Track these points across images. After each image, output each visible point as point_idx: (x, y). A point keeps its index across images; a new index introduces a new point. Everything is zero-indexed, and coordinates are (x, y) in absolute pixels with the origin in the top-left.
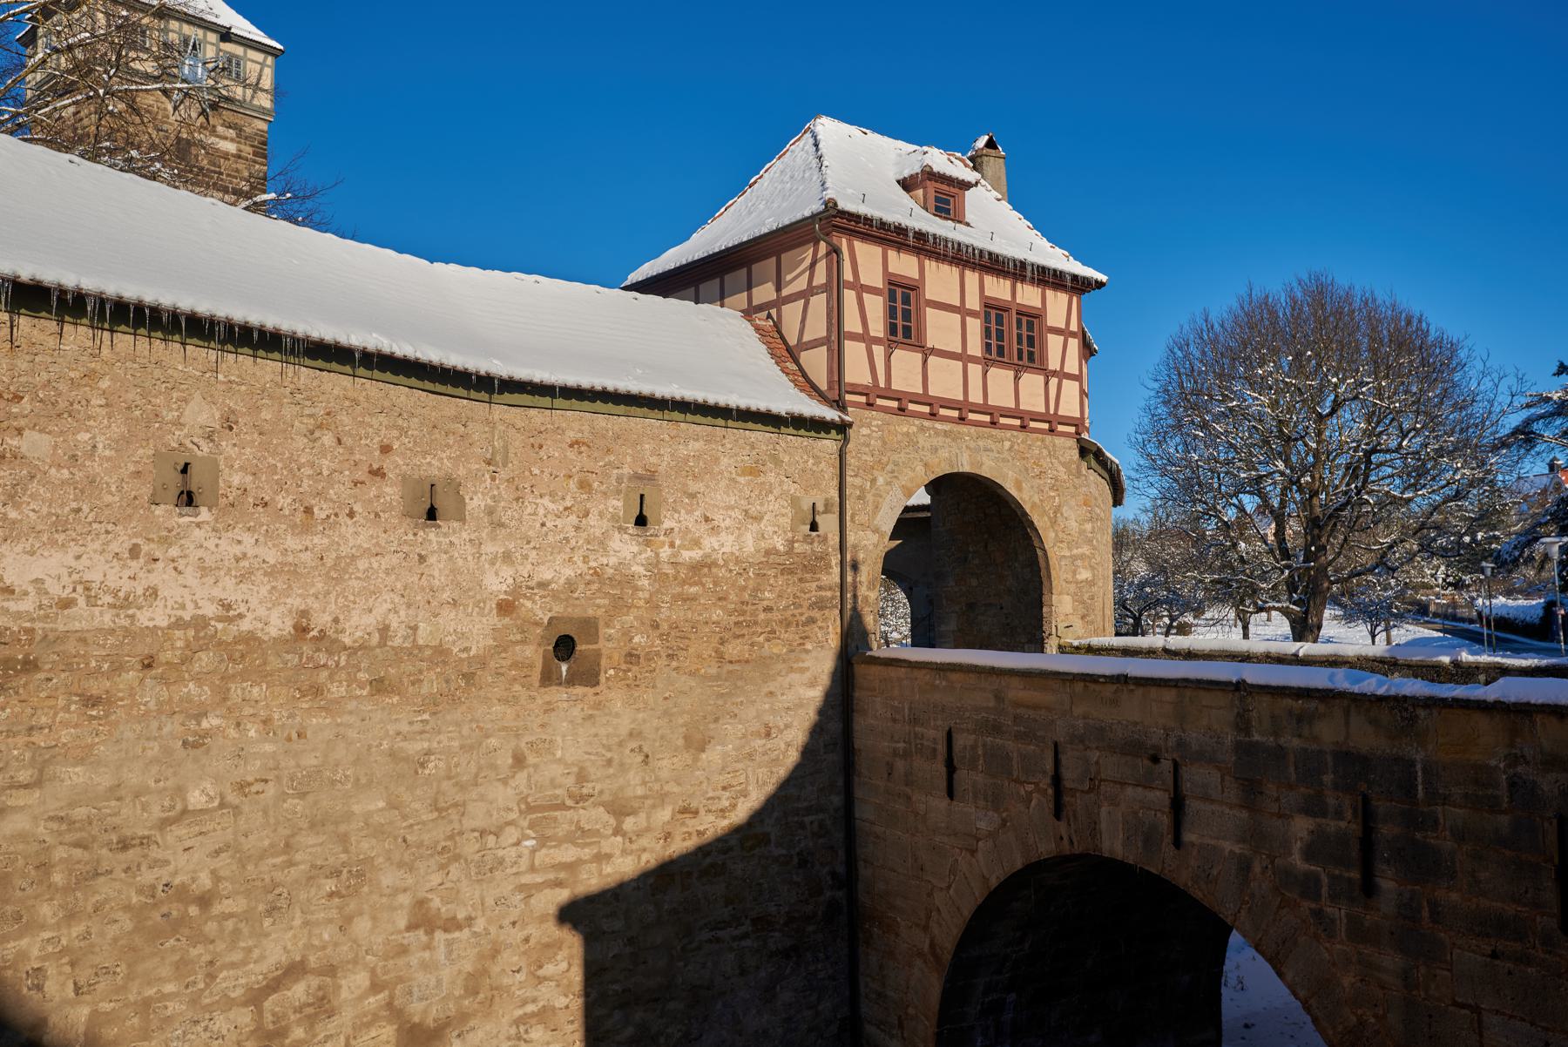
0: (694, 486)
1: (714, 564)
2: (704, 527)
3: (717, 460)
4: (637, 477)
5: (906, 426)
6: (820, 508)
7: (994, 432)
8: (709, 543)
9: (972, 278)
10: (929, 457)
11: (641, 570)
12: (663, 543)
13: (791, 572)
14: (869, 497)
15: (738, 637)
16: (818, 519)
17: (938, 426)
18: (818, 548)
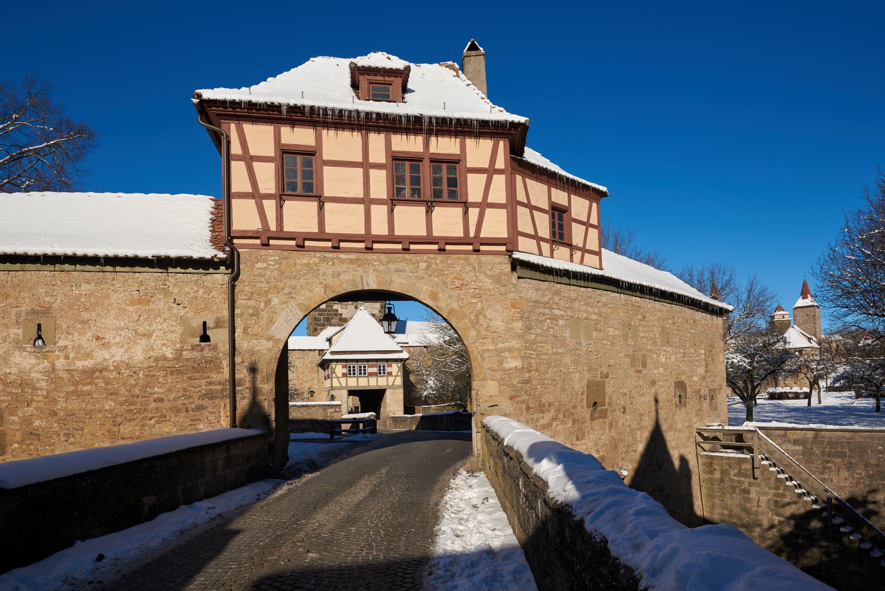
0: (85, 315)
1: (106, 369)
2: (95, 344)
3: (107, 297)
4: (33, 312)
5: (303, 259)
6: (210, 324)
7: (407, 256)
8: (101, 356)
9: (377, 140)
10: (330, 280)
11: (39, 376)
12: (58, 357)
13: (180, 372)
14: (264, 314)
15: (130, 420)
16: (208, 332)
17: (343, 256)
18: (208, 354)
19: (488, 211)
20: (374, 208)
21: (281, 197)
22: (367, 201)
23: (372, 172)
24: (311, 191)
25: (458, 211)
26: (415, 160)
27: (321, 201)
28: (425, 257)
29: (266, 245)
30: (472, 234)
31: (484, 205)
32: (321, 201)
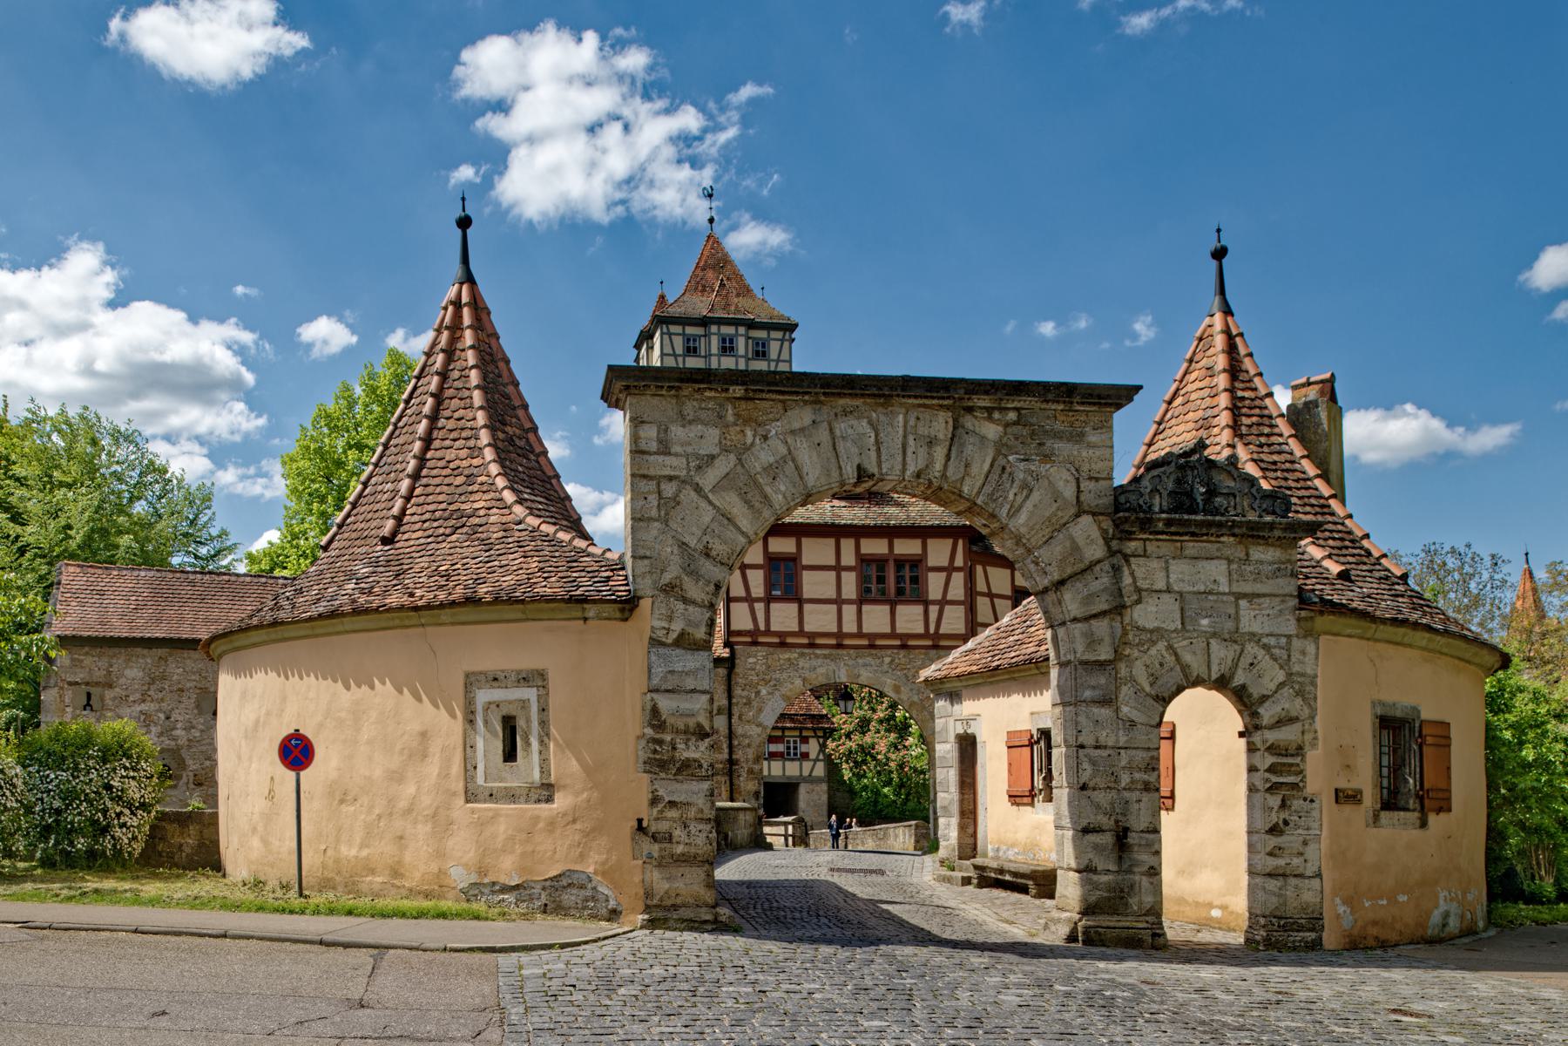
5: (786, 655)
9: (848, 545)
14: (755, 704)
17: (818, 652)
19: (947, 607)
20: (845, 607)
21: (769, 600)
22: (839, 602)
23: (844, 574)
24: (793, 594)
25: (919, 609)
26: (880, 562)
27: (800, 602)
28: (889, 652)
29: (755, 643)
30: (932, 631)
31: (943, 603)
32: (800, 602)
